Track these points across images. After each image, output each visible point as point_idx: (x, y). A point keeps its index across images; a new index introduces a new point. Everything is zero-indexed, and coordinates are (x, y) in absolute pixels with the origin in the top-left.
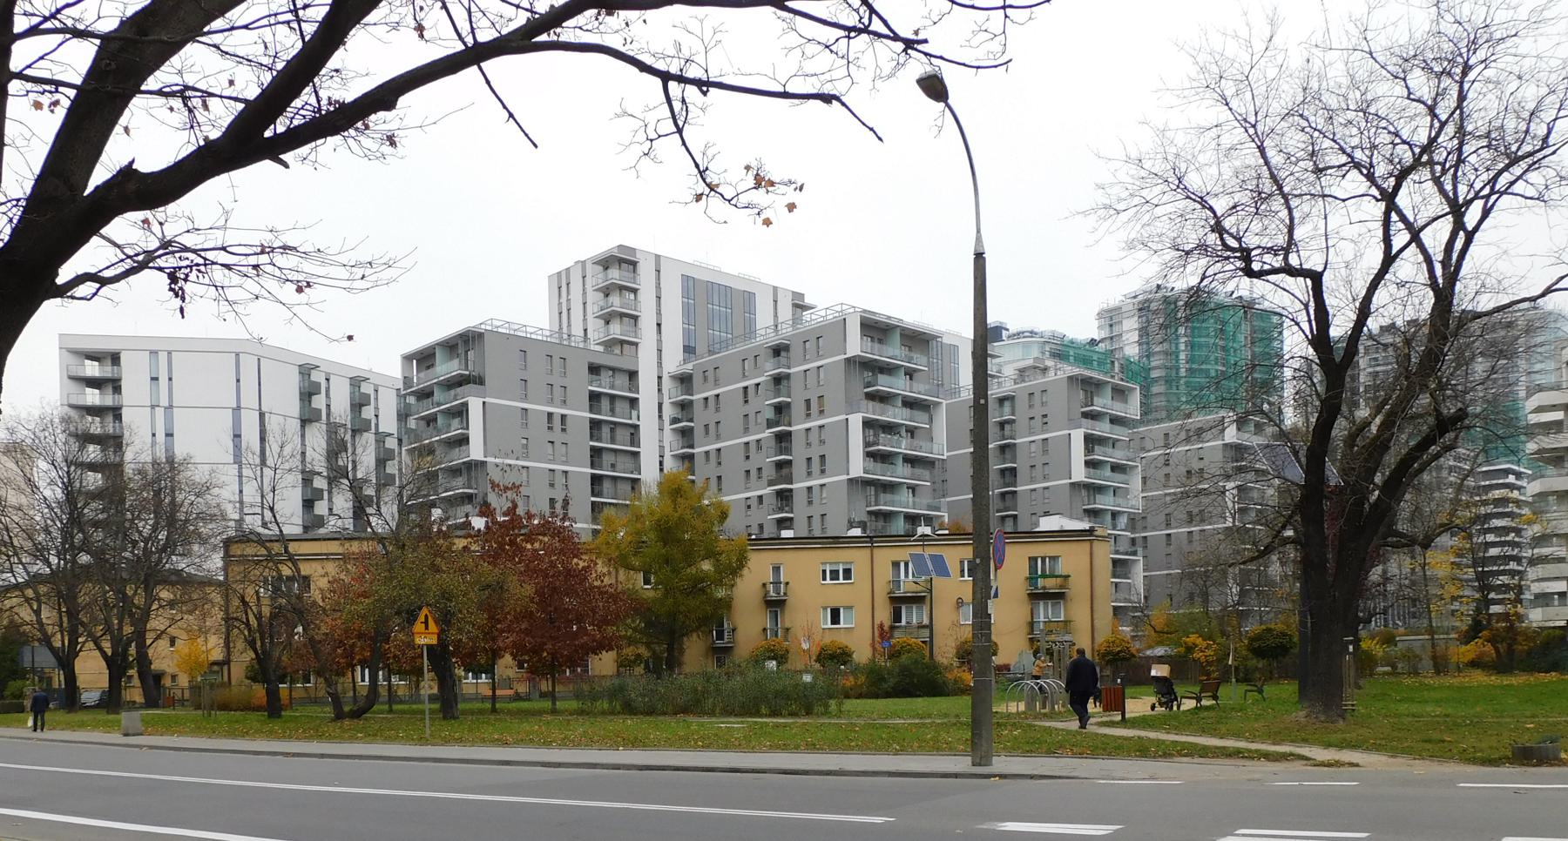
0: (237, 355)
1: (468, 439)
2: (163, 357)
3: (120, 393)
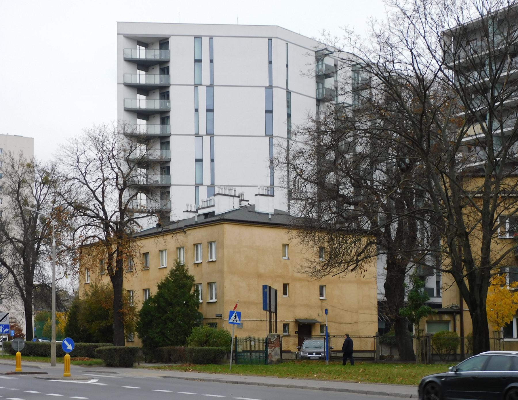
0: (270, 39)
1: (168, 43)
2: (206, 41)
3: (168, 73)
